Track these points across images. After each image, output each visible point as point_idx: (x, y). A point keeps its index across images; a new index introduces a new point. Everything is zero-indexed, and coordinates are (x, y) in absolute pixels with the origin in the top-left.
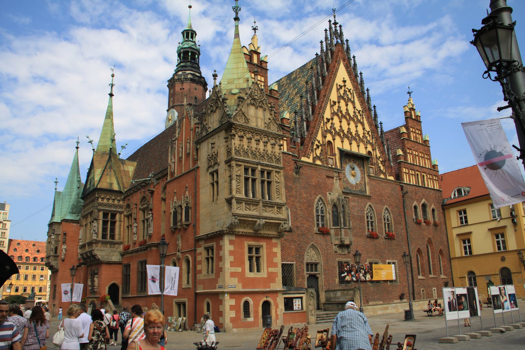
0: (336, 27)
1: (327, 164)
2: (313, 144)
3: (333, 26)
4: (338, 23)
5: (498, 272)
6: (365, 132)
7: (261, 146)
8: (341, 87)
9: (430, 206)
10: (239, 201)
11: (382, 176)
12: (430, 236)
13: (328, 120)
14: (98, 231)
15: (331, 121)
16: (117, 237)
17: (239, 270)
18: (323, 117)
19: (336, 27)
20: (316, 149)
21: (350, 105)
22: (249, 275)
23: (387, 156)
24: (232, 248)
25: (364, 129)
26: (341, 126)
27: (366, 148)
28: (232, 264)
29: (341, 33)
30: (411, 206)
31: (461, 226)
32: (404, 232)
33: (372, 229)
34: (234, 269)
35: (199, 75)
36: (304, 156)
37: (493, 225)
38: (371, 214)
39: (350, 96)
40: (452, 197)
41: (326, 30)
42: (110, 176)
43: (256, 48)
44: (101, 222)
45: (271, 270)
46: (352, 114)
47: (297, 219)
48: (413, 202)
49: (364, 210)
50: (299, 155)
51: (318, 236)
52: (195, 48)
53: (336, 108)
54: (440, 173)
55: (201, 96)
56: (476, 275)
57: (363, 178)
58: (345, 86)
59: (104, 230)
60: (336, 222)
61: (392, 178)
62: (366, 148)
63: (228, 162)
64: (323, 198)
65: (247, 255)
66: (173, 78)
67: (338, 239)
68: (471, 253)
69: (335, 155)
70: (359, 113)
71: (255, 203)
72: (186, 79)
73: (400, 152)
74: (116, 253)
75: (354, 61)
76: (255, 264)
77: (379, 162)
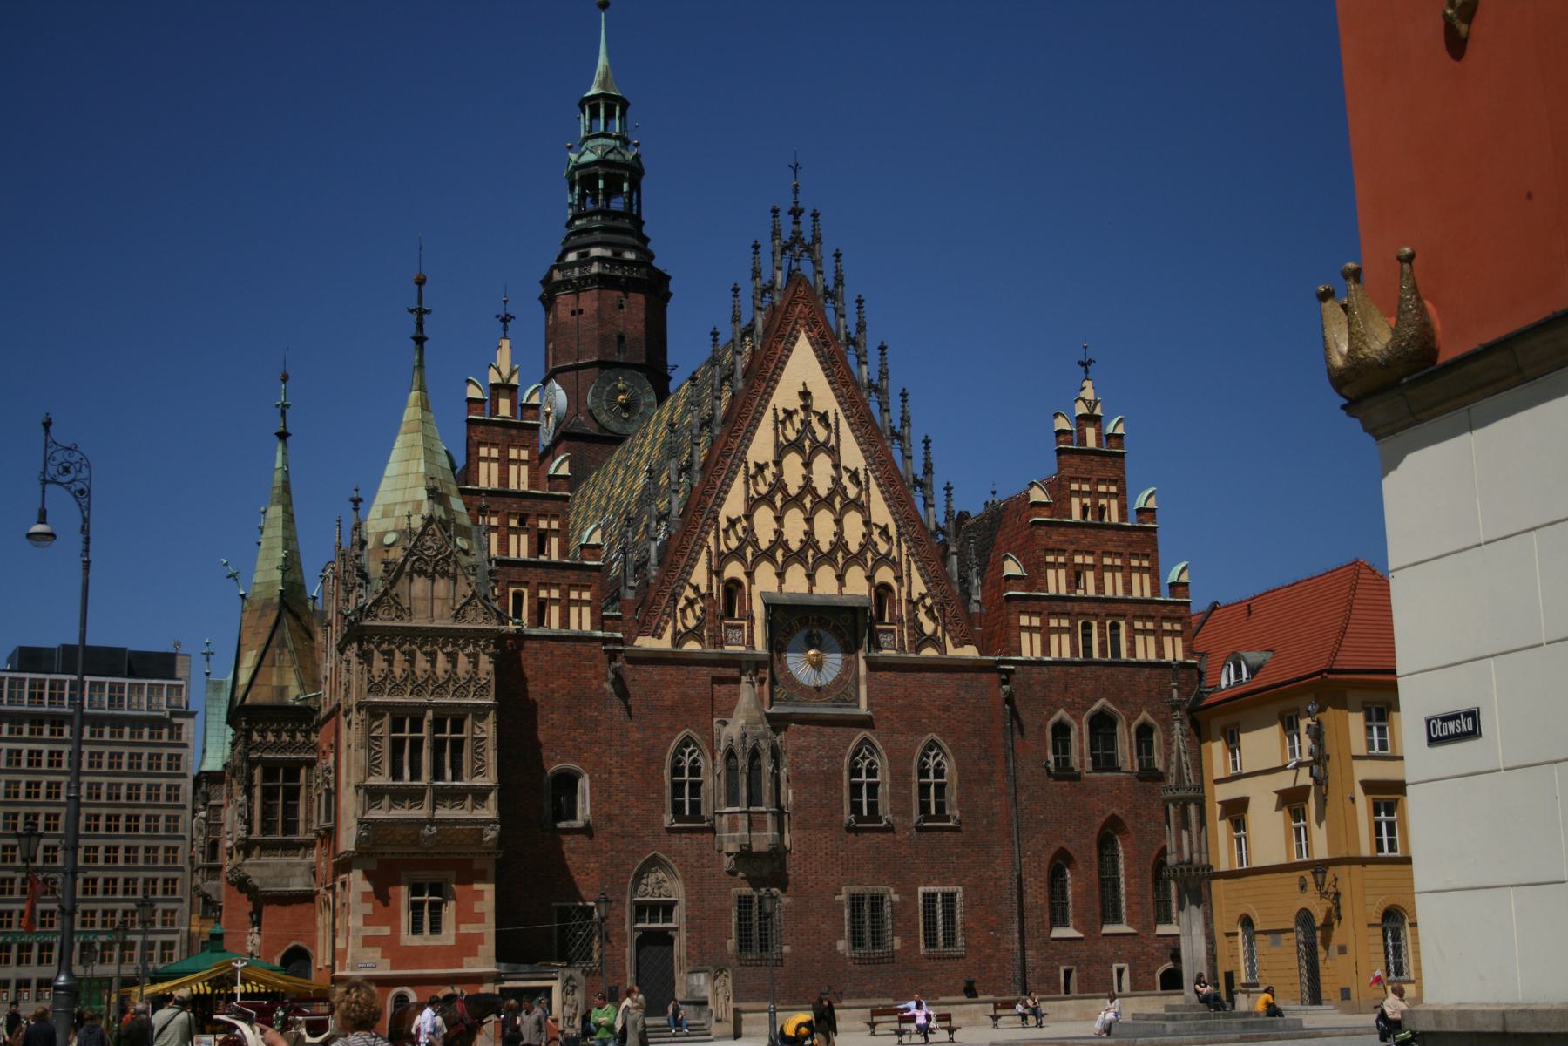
0: (797, 223)
1: (719, 642)
2: (675, 599)
4: (801, 211)
5: (1292, 925)
8: (789, 414)
10: (373, 795)
11: (929, 652)
12: (1115, 811)
13: (732, 523)
14: (250, 814)
16: (301, 826)
17: (386, 931)
18: (716, 519)
19: (797, 223)
20: (683, 611)
21: (822, 464)
22: (407, 939)
23: (957, 588)
25: (867, 523)
26: (778, 533)
28: (368, 920)
29: (817, 238)
30: (1042, 728)
33: (873, 807)
34: (371, 931)
35: (629, 255)
37: (1285, 781)
38: (871, 763)
40: (1224, 683)
42: (281, 667)
44: (257, 792)
45: (464, 929)
46: (823, 485)
47: (609, 797)
48: (1051, 714)
49: (842, 756)
51: (675, 840)
52: (619, 158)
54: (1194, 609)
55: (641, 327)
56: (1258, 928)
57: (849, 667)
58: (806, 408)
59: (268, 811)
60: (732, 799)
61: (970, 652)
62: (870, 578)
63: (360, 707)
64: (696, 737)
66: (550, 276)
67: (734, 839)
70: (854, 475)
71: (415, 796)
72: (585, 278)
73: (1012, 568)
74: (299, 871)
76: (427, 915)
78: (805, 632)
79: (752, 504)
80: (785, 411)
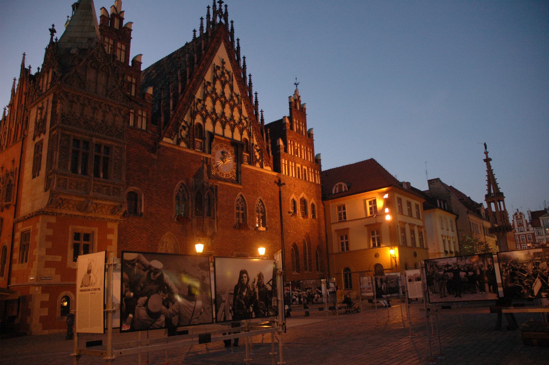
0: (220, 6)
3: (218, 5)
4: (223, 2)
6: (242, 118)
7: (99, 117)
8: (218, 67)
9: (310, 201)
13: (199, 101)
15: (202, 102)
17: (59, 258)
19: (220, 6)
24: (50, 232)
27: (241, 134)
29: (226, 13)
31: (339, 222)
32: (279, 225)
34: (50, 258)
36: (166, 137)
39: (228, 78)
40: (333, 192)
41: (209, 7)
43: (119, 12)
48: (291, 195)
50: (160, 135)
53: (209, 88)
58: (223, 67)
62: (241, 134)
65: (70, 242)
68: (347, 249)
69: (203, 139)
73: (281, 143)
75: (238, 44)
77: (255, 150)
78: (221, 150)
79: (205, 96)
80: (217, 66)
